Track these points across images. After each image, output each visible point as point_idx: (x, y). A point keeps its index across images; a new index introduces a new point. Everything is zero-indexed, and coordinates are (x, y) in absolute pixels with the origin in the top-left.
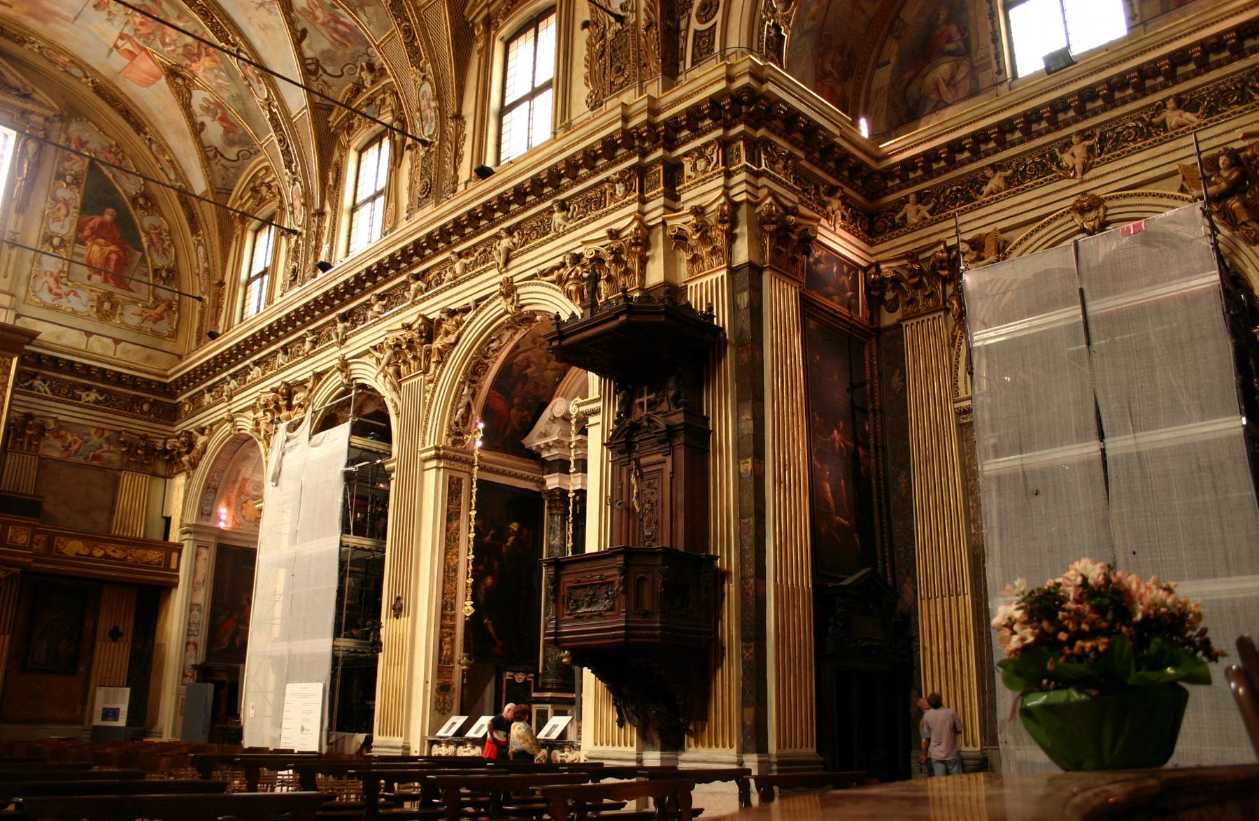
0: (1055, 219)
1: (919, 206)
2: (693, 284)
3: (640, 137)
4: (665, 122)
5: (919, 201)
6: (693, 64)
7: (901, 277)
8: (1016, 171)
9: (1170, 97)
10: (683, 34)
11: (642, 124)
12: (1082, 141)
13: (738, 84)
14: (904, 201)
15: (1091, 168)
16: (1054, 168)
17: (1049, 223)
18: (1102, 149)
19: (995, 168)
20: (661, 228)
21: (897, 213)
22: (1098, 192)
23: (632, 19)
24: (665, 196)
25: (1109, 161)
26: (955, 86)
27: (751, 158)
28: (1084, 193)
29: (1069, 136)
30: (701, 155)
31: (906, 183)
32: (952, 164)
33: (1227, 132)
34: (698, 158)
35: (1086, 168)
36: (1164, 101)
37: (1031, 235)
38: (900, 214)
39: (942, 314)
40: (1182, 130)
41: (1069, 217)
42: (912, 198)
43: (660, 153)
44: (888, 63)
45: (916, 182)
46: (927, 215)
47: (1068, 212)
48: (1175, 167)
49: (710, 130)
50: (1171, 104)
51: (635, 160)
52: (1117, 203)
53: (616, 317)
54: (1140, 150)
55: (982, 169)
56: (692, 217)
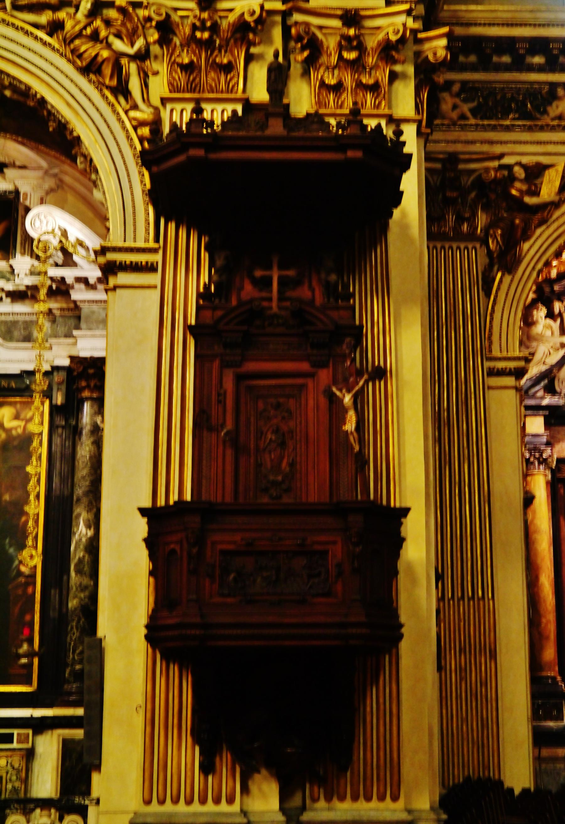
1: (457, 101)
32: (519, 65)
42: (456, 88)
46: (469, 114)
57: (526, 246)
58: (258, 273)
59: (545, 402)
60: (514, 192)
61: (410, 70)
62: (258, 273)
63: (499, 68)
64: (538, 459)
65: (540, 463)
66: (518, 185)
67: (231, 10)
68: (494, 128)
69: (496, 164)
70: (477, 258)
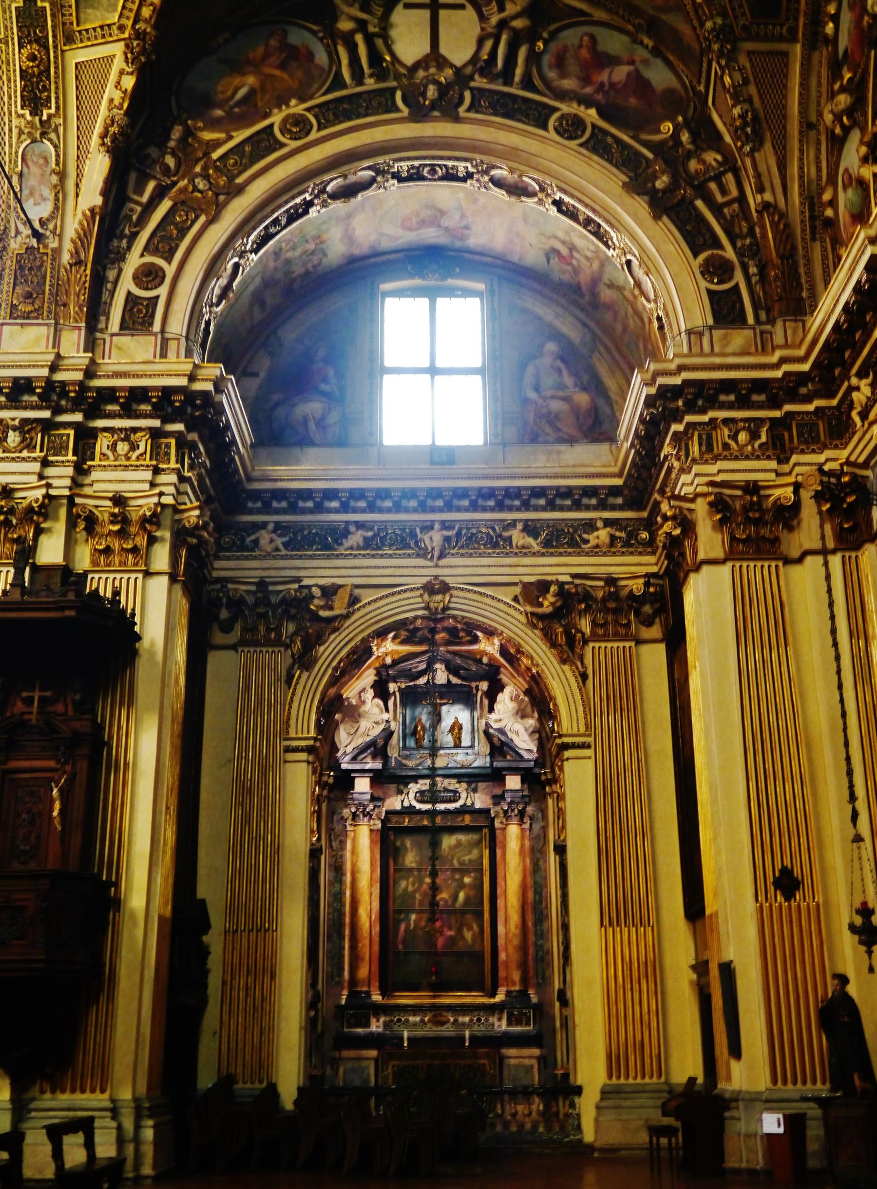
0: (405, 591)
1: (274, 536)
2: (97, 576)
3: (64, 394)
4: (99, 390)
6: (122, 327)
7: (246, 601)
8: (375, 536)
9: (521, 520)
10: (109, 286)
11: (73, 383)
12: (441, 529)
13: (198, 386)
14: (264, 525)
15: (445, 557)
16: (412, 545)
17: (399, 593)
18: (457, 542)
19: (360, 525)
20: (65, 501)
21: (249, 535)
22: (448, 580)
23: (53, 244)
24: (75, 467)
26: (324, 428)
27: (180, 460)
29: (433, 521)
30: (127, 439)
31: (267, 509)
32: (319, 508)
33: (557, 565)
34: (122, 440)
35: (441, 556)
36: (515, 521)
37: (381, 598)
38: (253, 537)
39: (282, 649)
41: (418, 593)
42: (271, 527)
43: (78, 417)
44: (255, 375)
45: (277, 512)
46: (281, 547)
47: (418, 589)
48: (516, 579)
49: (145, 416)
50: (520, 526)
51: (46, 414)
52: (461, 594)
53: (62, 609)
55: (347, 523)
56: (109, 503)
57: (322, 649)
58: (25, 694)
59: (368, 767)
61: (167, 535)
62: (25, 694)
63: (304, 511)
64: (363, 812)
65: (364, 816)
66: (316, 602)
67: (24, 498)
68: (300, 557)
69: (296, 586)
70: (282, 659)
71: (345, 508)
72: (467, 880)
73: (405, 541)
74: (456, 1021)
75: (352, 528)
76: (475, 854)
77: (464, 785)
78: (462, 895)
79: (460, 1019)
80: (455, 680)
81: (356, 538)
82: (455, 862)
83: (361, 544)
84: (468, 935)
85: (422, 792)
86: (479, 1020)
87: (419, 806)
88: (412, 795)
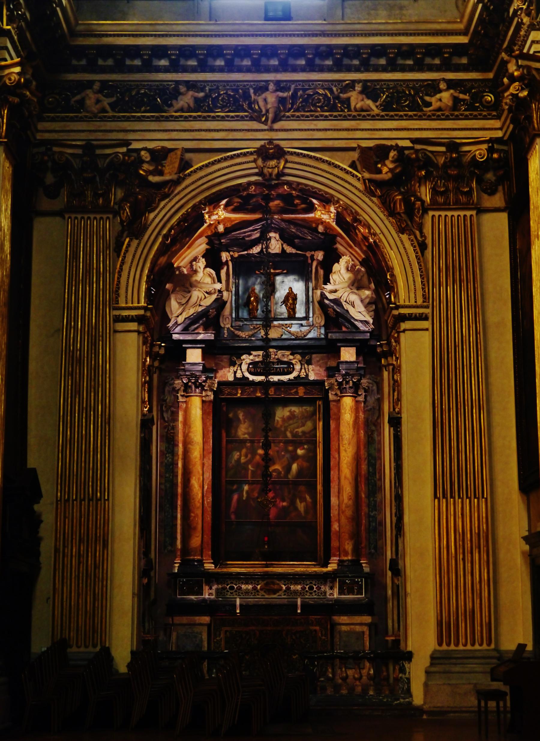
0: (238, 156)
5: (100, 91)
8: (207, 96)
9: (359, 81)
14: (90, 84)
17: (232, 157)
19: (191, 85)
21: (74, 95)
22: (283, 144)
25: (298, 119)
28: (270, 141)
32: (148, 67)
35: (276, 120)
36: (354, 82)
38: (78, 97)
39: (111, 216)
40: (364, 114)
41: (251, 158)
42: (96, 86)
45: (104, 70)
46: (108, 108)
47: (251, 153)
48: (354, 144)
50: (358, 88)
52: (297, 159)
54: (326, 118)
55: (178, 83)
57: (152, 215)
59: (200, 337)
60: (141, 172)
63: (133, 70)
64: (194, 383)
65: (197, 387)
66: (146, 166)
68: (128, 119)
69: (124, 150)
70: (109, 226)
71: (175, 67)
72: (300, 452)
73: (238, 102)
74: (288, 589)
75: (183, 89)
76: (309, 425)
77: (298, 357)
78: (295, 467)
79: (292, 587)
80: (289, 250)
81: (187, 99)
82: (289, 434)
83: (192, 105)
84: (301, 506)
85: (254, 364)
86: (311, 588)
87: (251, 378)
88: (244, 367)
